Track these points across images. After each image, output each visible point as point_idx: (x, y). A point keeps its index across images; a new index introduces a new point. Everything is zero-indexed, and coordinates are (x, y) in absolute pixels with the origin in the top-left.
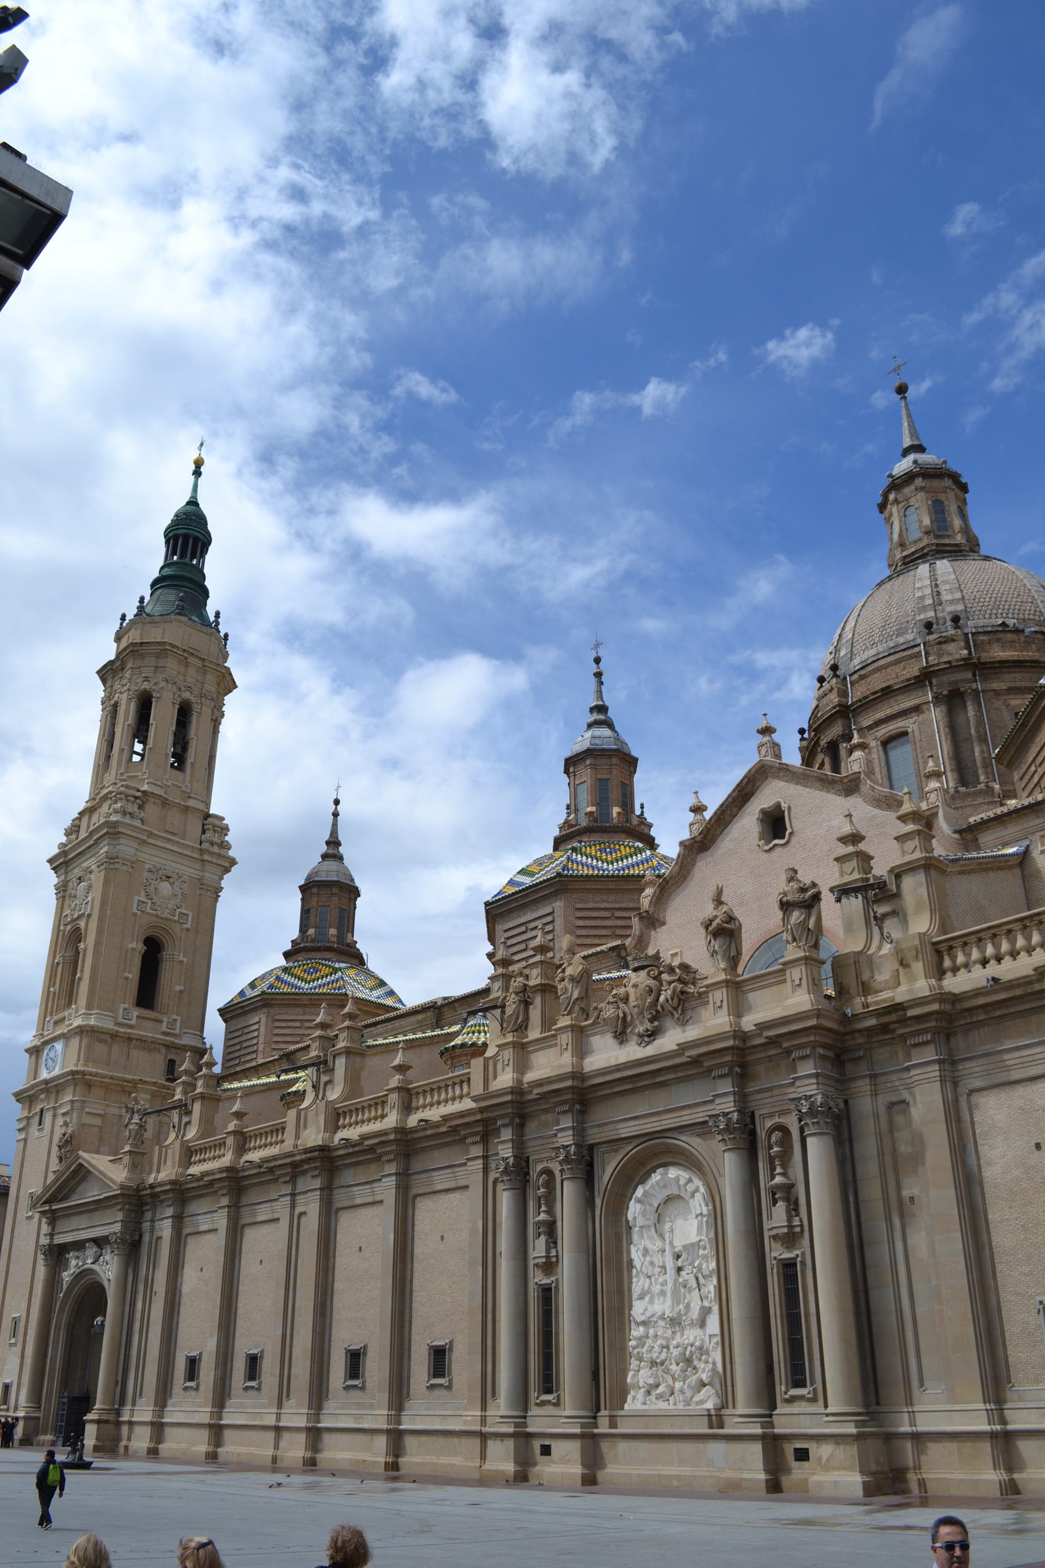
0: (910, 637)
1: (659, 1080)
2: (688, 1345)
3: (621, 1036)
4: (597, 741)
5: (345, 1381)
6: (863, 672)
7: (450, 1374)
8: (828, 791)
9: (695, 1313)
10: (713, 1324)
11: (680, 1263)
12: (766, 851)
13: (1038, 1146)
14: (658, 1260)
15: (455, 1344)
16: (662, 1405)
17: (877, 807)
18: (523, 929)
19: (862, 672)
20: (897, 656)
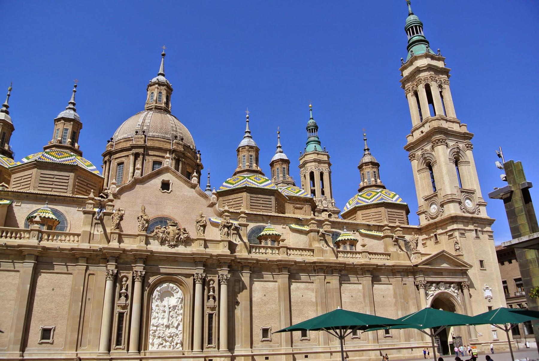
0: (169, 136)
1: (177, 259)
2: (172, 333)
3: (162, 243)
4: (76, 117)
5: (41, 340)
6: (153, 138)
7: (53, 338)
8: (185, 184)
9: (176, 325)
10: (180, 328)
11: (170, 310)
12: (162, 192)
13: (265, 295)
14: (162, 308)
15: (56, 328)
16: (164, 349)
17: (199, 195)
18: (52, 176)
19: (152, 138)
20: (164, 140)
